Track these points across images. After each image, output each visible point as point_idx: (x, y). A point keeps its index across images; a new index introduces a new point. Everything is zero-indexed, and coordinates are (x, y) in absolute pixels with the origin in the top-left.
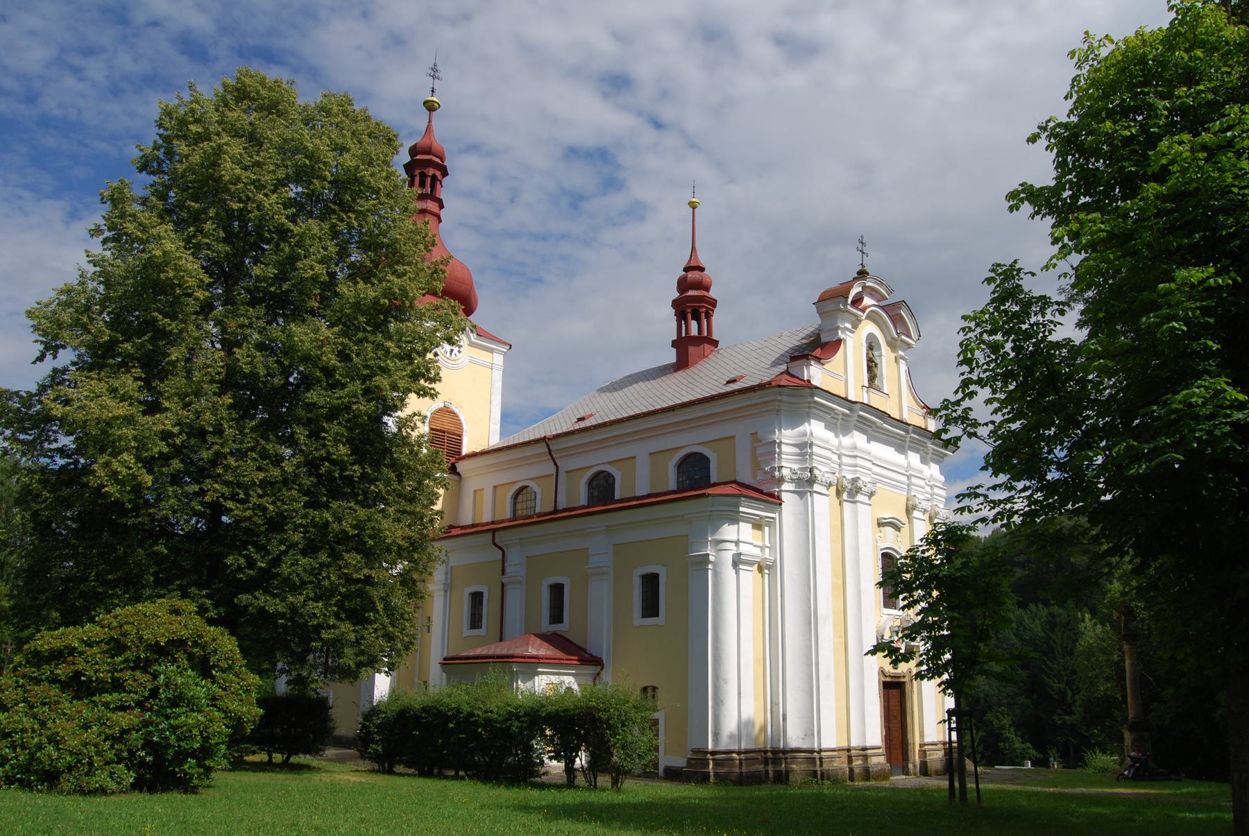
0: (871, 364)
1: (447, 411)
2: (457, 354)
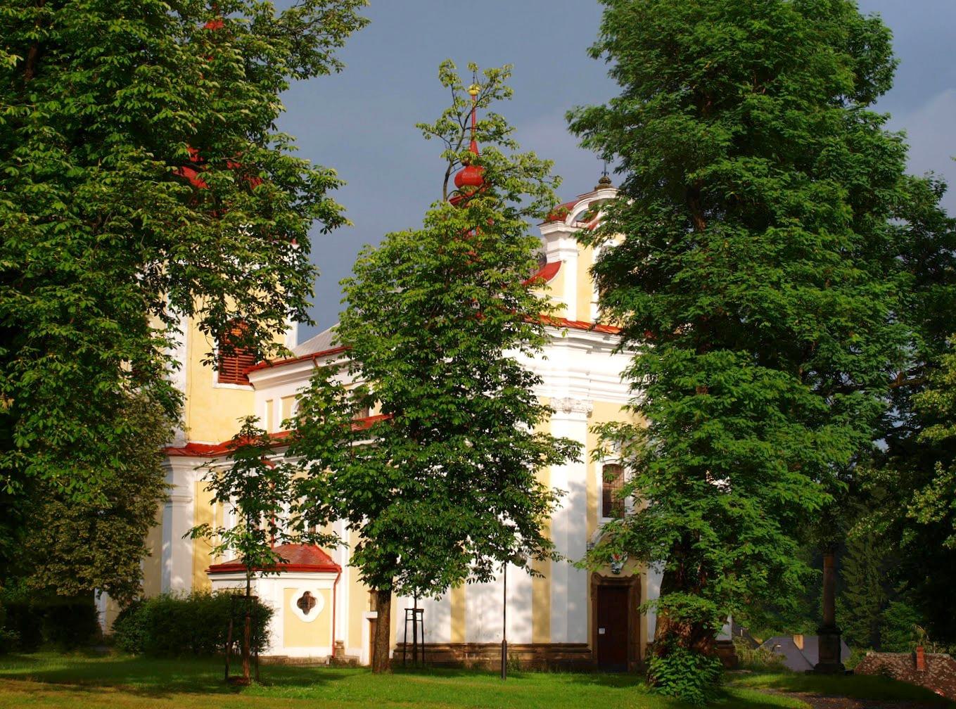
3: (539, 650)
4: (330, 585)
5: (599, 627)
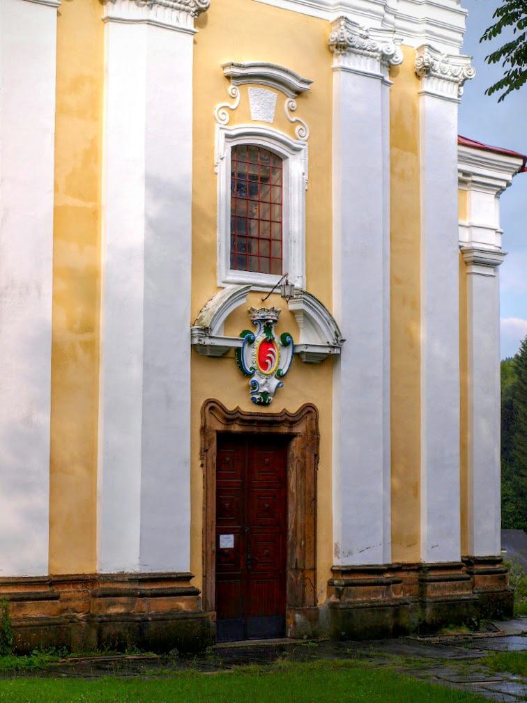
3: (68, 591)
5: (220, 532)
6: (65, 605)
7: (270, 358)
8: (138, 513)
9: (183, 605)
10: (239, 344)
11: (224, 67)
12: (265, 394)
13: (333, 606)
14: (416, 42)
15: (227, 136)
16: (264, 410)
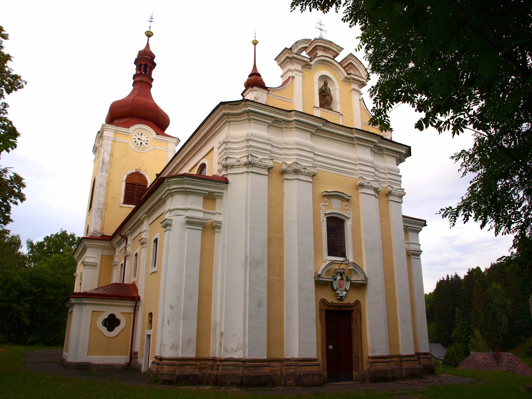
0: (324, 94)
1: (138, 174)
2: (145, 145)
3: (273, 364)
4: (131, 310)
6: (273, 369)
7: (342, 285)
8: (298, 337)
9: (315, 369)
10: (332, 280)
11: (322, 193)
12: (341, 297)
13: (369, 371)
14: (386, 186)
15: (325, 214)
16: (342, 302)
